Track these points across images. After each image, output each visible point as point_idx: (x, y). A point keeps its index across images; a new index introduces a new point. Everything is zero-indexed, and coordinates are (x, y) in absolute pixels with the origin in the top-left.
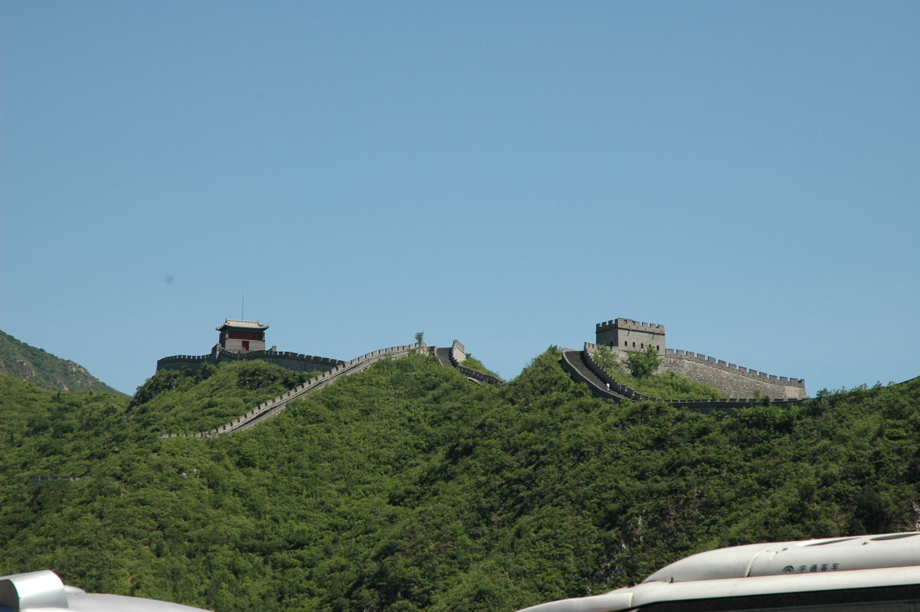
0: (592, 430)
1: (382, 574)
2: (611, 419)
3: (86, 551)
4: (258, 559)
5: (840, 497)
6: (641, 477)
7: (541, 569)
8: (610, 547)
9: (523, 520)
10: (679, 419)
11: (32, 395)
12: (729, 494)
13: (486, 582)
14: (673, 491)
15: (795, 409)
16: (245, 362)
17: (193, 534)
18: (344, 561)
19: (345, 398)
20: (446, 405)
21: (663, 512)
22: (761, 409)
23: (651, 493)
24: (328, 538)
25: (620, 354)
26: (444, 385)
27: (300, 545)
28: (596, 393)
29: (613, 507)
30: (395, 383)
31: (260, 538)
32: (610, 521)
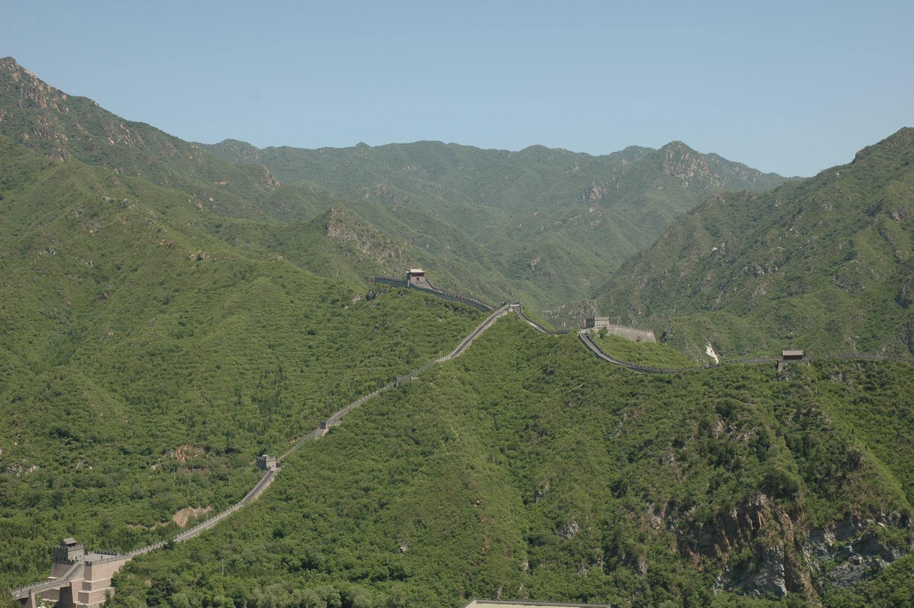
1: (535, 425)
2: (608, 372)
3: (433, 416)
4: (485, 412)
5: (695, 418)
6: (622, 396)
7: (594, 431)
8: (616, 423)
9: (584, 410)
10: (632, 374)
11: (316, 281)
12: (653, 408)
13: (579, 437)
14: (635, 405)
15: (672, 375)
16: (426, 294)
17: (463, 405)
18: (515, 414)
19: (493, 337)
20: (531, 341)
22: (662, 375)
23: (627, 404)
24: (505, 401)
25: (596, 329)
26: (527, 331)
27: (496, 405)
28: (598, 356)
29: (614, 407)
30: (508, 328)
31: (483, 403)
32: (614, 412)
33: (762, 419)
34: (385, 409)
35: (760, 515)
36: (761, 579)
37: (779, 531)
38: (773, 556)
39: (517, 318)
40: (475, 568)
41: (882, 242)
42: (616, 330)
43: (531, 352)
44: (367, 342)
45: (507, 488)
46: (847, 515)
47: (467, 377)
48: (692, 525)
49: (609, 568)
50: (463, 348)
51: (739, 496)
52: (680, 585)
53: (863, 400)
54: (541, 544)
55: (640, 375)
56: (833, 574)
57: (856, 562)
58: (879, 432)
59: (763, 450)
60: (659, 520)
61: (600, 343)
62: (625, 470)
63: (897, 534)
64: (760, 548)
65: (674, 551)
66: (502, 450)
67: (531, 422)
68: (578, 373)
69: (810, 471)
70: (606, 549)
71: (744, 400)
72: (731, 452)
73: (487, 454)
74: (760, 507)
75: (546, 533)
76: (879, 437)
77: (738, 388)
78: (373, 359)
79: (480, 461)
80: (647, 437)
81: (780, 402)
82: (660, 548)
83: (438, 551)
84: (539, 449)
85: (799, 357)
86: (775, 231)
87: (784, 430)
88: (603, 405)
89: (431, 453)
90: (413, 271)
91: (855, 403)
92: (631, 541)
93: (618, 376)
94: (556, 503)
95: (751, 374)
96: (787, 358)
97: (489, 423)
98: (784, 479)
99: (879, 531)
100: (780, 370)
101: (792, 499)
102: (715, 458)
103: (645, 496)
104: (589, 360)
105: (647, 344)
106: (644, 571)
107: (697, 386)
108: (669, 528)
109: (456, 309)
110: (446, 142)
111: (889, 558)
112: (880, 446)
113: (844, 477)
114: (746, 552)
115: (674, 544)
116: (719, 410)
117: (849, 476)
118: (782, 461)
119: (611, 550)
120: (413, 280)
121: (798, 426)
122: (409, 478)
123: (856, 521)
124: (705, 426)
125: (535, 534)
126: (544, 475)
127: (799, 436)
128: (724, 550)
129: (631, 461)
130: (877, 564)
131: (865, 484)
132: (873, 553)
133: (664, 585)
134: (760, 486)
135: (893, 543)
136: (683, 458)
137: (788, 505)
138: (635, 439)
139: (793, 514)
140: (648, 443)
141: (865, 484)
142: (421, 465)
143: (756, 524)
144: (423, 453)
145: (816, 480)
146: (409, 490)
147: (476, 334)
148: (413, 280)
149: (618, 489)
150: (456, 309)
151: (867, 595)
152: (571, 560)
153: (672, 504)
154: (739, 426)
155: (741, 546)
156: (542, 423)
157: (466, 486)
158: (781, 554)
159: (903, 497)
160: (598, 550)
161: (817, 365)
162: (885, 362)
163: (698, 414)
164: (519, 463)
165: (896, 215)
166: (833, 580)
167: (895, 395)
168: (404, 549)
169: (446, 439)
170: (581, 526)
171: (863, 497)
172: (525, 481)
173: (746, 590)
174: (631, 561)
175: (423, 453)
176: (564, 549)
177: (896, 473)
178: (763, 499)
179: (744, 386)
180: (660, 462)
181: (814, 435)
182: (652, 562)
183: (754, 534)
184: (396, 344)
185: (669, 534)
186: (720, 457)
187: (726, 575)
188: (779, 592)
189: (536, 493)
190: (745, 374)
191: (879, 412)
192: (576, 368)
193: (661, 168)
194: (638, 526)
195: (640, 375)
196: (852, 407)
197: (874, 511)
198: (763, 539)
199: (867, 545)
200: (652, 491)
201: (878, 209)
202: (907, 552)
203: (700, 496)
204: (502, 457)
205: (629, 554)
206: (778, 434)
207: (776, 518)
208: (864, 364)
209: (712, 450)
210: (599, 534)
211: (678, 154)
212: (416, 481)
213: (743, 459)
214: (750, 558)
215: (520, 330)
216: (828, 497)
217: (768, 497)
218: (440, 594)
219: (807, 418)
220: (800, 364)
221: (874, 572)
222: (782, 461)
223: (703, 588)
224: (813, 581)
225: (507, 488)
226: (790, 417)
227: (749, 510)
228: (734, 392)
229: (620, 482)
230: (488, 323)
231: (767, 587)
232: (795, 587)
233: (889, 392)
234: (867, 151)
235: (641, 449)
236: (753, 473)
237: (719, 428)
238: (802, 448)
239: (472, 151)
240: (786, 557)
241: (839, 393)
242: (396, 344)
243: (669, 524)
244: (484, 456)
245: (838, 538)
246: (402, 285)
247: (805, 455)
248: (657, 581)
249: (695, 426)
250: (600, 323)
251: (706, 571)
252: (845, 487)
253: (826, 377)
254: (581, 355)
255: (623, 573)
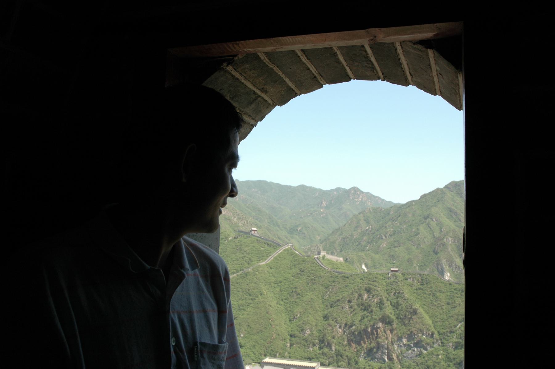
0: (322, 274)
8: (327, 292)
9: (315, 286)
13: (312, 297)
21: (333, 288)
25: (321, 256)
32: (326, 288)
33: (382, 294)
34: (238, 281)
35: (379, 331)
36: (378, 355)
37: (386, 337)
38: (383, 347)
39: (291, 249)
40: (269, 345)
41: (429, 229)
42: (329, 257)
43: (296, 263)
44: (234, 255)
45: (283, 315)
46: (411, 332)
47: (271, 271)
48: (353, 333)
49: (320, 348)
50: (270, 259)
51: (372, 323)
52: (347, 356)
53: (420, 289)
54: (295, 337)
55: (337, 274)
56: (405, 355)
57: (414, 351)
58: (425, 301)
59: (381, 306)
60: (341, 330)
61: (322, 261)
62: (329, 310)
63: (429, 340)
64: (378, 343)
65: (346, 343)
66: (282, 300)
67: (294, 290)
68: (313, 272)
69: (399, 315)
70: (320, 340)
71: (375, 286)
72: (370, 306)
73: (276, 301)
74: (379, 328)
75: (297, 333)
76: (425, 303)
77: (373, 281)
78: (235, 262)
79: (274, 303)
80: (338, 298)
81: (389, 288)
82: (341, 341)
83: (255, 337)
84: (297, 300)
85: (396, 271)
86: (390, 223)
87: (390, 299)
88: (322, 285)
89: (255, 299)
90: (253, 229)
91: (416, 289)
92: (329, 338)
93: (328, 274)
94: (302, 321)
95: (379, 277)
96: (392, 271)
97: (278, 289)
98: (389, 317)
99: (423, 339)
100: (390, 275)
101: (391, 325)
102: (363, 308)
103: (336, 321)
104: (317, 267)
105: (340, 263)
106: (334, 350)
107: (358, 280)
108: (344, 334)
109: (268, 245)
110: (269, 181)
111: (426, 349)
112: (425, 307)
113: (411, 318)
114: (373, 345)
115: (346, 340)
116: (366, 289)
117: (413, 317)
118: (389, 311)
119: (322, 341)
120: (253, 232)
121: (395, 297)
122: (246, 309)
123: (415, 335)
124: (360, 295)
125: (292, 333)
126: (298, 310)
127: (395, 301)
128: (365, 343)
129: (331, 307)
130: (421, 352)
131: (419, 321)
132: (420, 347)
133: (341, 356)
134: (380, 319)
135: (428, 344)
136: (351, 307)
137: (390, 327)
138: (333, 299)
139: (391, 331)
140: (338, 300)
141: (419, 321)
142: (251, 304)
143: (377, 334)
144: (252, 299)
145: (401, 318)
146: (246, 313)
147: (275, 254)
148: (253, 232)
149: (326, 317)
150: (268, 245)
151: (417, 363)
152: (305, 344)
153: (346, 325)
154: (373, 296)
155: (371, 342)
156: (298, 290)
157: (267, 313)
158: (386, 346)
159: (432, 327)
160: (317, 341)
161: (403, 274)
162: (428, 275)
163: (358, 291)
164: (288, 305)
165: (434, 220)
166: (405, 357)
167: (431, 287)
168: (242, 335)
169: (261, 294)
170: (311, 331)
171: (418, 326)
172: (290, 312)
173: (372, 359)
174: (329, 345)
175: (252, 299)
176: (303, 340)
177: (430, 317)
178: (380, 324)
179: (375, 281)
180: (343, 308)
181: (401, 301)
182: (337, 347)
183: (376, 338)
184: (244, 257)
185: (344, 336)
186: (365, 308)
187: (364, 353)
188: (384, 361)
189: (294, 318)
190: (376, 276)
191: (425, 294)
192: (312, 270)
193: (349, 197)
194: (332, 332)
195: (337, 274)
196: (415, 291)
197: (421, 331)
198: (380, 340)
199: (418, 344)
200: (339, 319)
201: (428, 217)
202: (433, 347)
203: (357, 322)
204: (282, 303)
205: (328, 343)
206: (387, 300)
207: (385, 332)
208: (420, 275)
209: (362, 305)
210: (318, 334)
211: (355, 191)
212: (248, 310)
213: (374, 309)
214: (374, 347)
215: (292, 254)
216: (405, 325)
217: (383, 324)
218: (255, 354)
219: (398, 294)
220: (397, 274)
221: (420, 354)
222: (389, 311)
223: (356, 358)
224: (398, 357)
225: (283, 315)
226: (392, 294)
227: (375, 328)
228: (372, 283)
229: (327, 315)
230: (280, 251)
231: (380, 359)
232: (390, 359)
233: (429, 286)
234: (425, 194)
235: (335, 303)
236: (377, 314)
237: (366, 296)
238: (396, 306)
239: (278, 185)
240: (388, 348)
241: (411, 285)
242: (244, 257)
243: (344, 332)
244: (275, 302)
245: (408, 341)
246: (248, 233)
247: (397, 308)
248: (339, 354)
249: (356, 295)
250: (323, 253)
251: (358, 351)
252: (411, 322)
253: (406, 279)
254: (315, 265)
255: (326, 350)
